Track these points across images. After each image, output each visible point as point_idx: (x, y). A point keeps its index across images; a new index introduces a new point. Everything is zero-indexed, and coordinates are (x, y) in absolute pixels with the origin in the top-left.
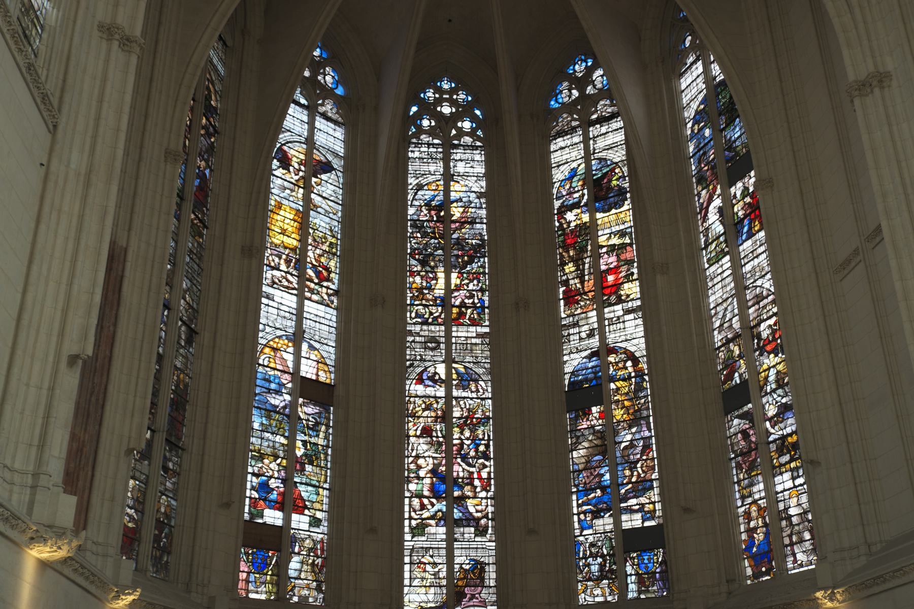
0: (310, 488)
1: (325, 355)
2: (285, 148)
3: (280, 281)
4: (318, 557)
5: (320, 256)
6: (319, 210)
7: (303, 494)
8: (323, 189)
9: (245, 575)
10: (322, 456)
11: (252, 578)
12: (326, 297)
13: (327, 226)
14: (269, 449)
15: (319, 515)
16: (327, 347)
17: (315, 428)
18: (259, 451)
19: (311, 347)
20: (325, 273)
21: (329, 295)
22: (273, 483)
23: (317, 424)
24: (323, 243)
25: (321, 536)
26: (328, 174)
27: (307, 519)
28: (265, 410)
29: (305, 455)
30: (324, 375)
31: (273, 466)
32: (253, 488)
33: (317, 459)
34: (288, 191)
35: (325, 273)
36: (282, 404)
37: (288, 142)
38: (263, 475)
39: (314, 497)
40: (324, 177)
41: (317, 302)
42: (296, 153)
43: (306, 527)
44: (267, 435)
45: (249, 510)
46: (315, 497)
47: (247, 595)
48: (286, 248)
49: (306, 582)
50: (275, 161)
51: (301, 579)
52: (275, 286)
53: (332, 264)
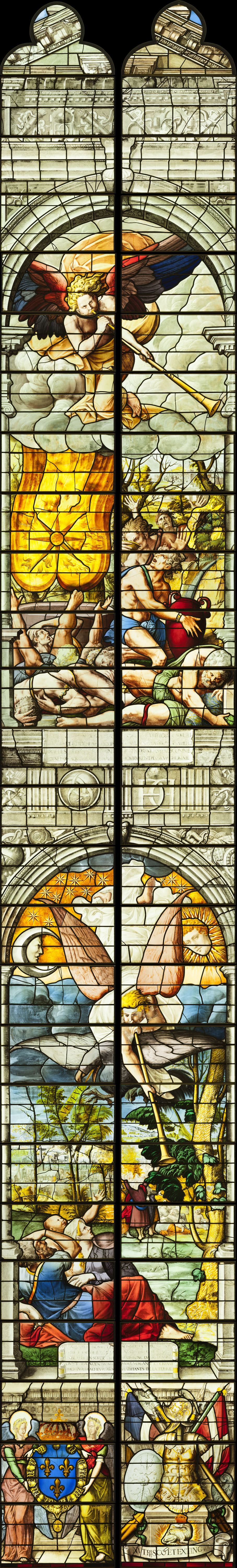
0: (176, 1268)
1: (200, 876)
2: (45, 261)
3: (58, 701)
4: (210, 1443)
5: (167, 573)
6: (157, 422)
7: (155, 1287)
8: (166, 343)
9: (20, 1511)
10: (208, 1171)
11: (40, 1515)
12: (195, 701)
13: (188, 466)
14: (61, 1187)
15: (206, 1334)
16: (207, 853)
17: (183, 1099)
18: (32, 1200)
19: (158, 869)
20: (189, 624)
21: (202, 690)
22: (78, 1275)
23: (188, 1085)
24: (176, 529)
25: (215, 1388)
26: (183, 286)
27: (171, 1351)
28: (42, 1083)
29: (154, 1179)
30: (201, 939)
31: (75, 1227)
32: (21, 1297)
33: (191, 1182)
34: (62, 405)
35: (189, 624)
36: (92, 1057)
37: (50, 239)
38: (47, 1258)
39: (189, 1289)
40: (166, 301)
41: (166, 725)
42: (80, 264)
43: (172, 1370)
44: (52, 1151)
45: (16, 1350)
46: (194, 1287)
47: (31, 1557)
48: (67, 589)
49: (177, 1508)
50: (14, 320)
51: (160, 1502)
52: (46, 720)
53: (210, 586)
